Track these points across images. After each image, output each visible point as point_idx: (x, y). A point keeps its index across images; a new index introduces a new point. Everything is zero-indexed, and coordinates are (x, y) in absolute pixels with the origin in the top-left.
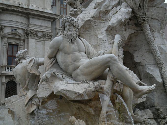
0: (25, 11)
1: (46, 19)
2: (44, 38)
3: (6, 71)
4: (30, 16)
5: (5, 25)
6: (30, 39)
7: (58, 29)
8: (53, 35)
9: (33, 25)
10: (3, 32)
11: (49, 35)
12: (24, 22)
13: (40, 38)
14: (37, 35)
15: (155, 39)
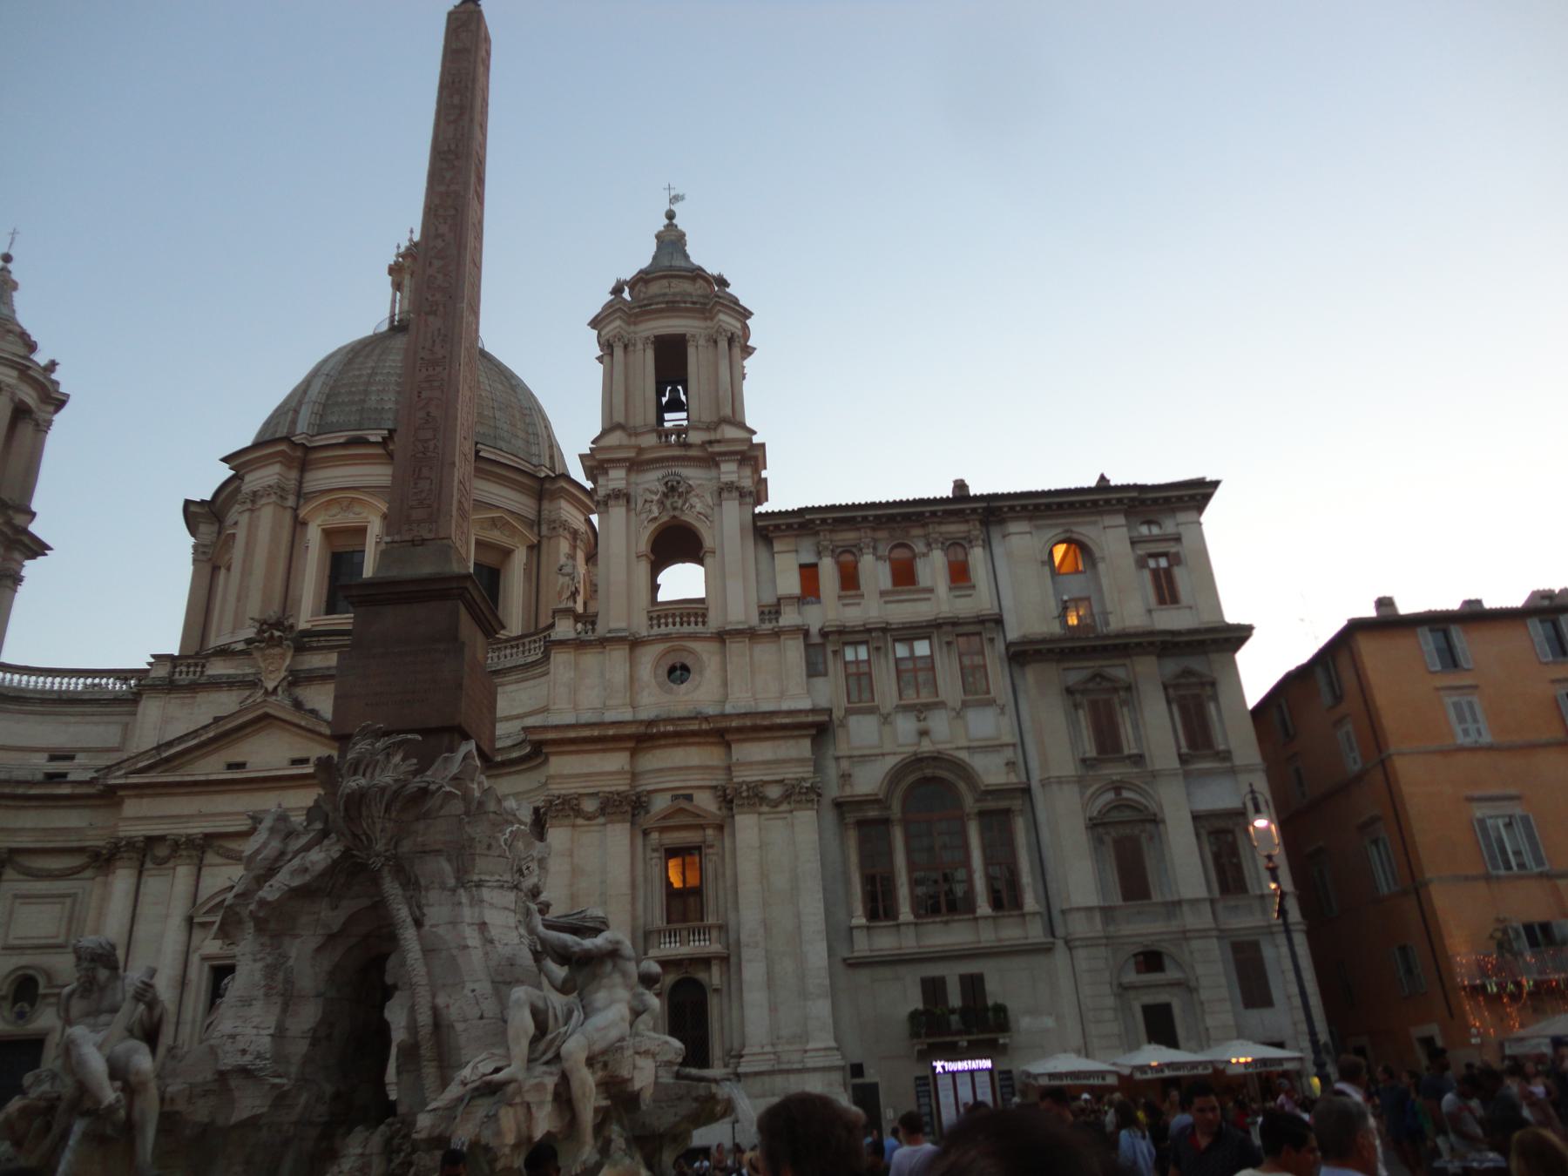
0: (705, 726)
1: (788, 733)
2: (789, 803)
3: (662, 946)
4: (728, 737)
5: (650, 788)
6: (737, 818)
7: (843, 757)
8: (820, 785)
9: (743, 764)
10: (647, 812)
11: (807, 788)
12: (715, 763)
13: (776, 806)
14: (763, 799)
15: (426, 910)
